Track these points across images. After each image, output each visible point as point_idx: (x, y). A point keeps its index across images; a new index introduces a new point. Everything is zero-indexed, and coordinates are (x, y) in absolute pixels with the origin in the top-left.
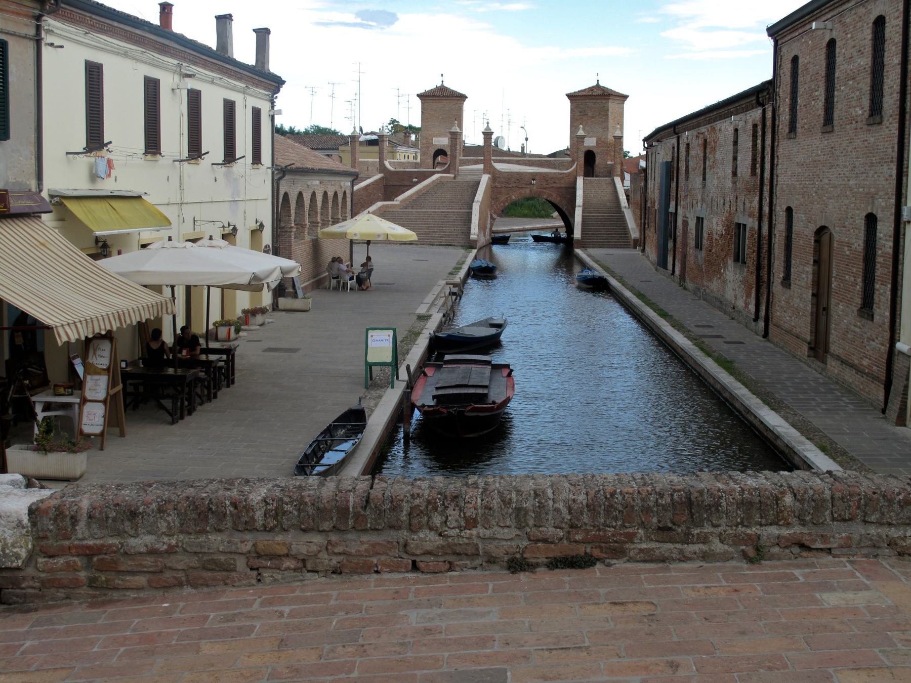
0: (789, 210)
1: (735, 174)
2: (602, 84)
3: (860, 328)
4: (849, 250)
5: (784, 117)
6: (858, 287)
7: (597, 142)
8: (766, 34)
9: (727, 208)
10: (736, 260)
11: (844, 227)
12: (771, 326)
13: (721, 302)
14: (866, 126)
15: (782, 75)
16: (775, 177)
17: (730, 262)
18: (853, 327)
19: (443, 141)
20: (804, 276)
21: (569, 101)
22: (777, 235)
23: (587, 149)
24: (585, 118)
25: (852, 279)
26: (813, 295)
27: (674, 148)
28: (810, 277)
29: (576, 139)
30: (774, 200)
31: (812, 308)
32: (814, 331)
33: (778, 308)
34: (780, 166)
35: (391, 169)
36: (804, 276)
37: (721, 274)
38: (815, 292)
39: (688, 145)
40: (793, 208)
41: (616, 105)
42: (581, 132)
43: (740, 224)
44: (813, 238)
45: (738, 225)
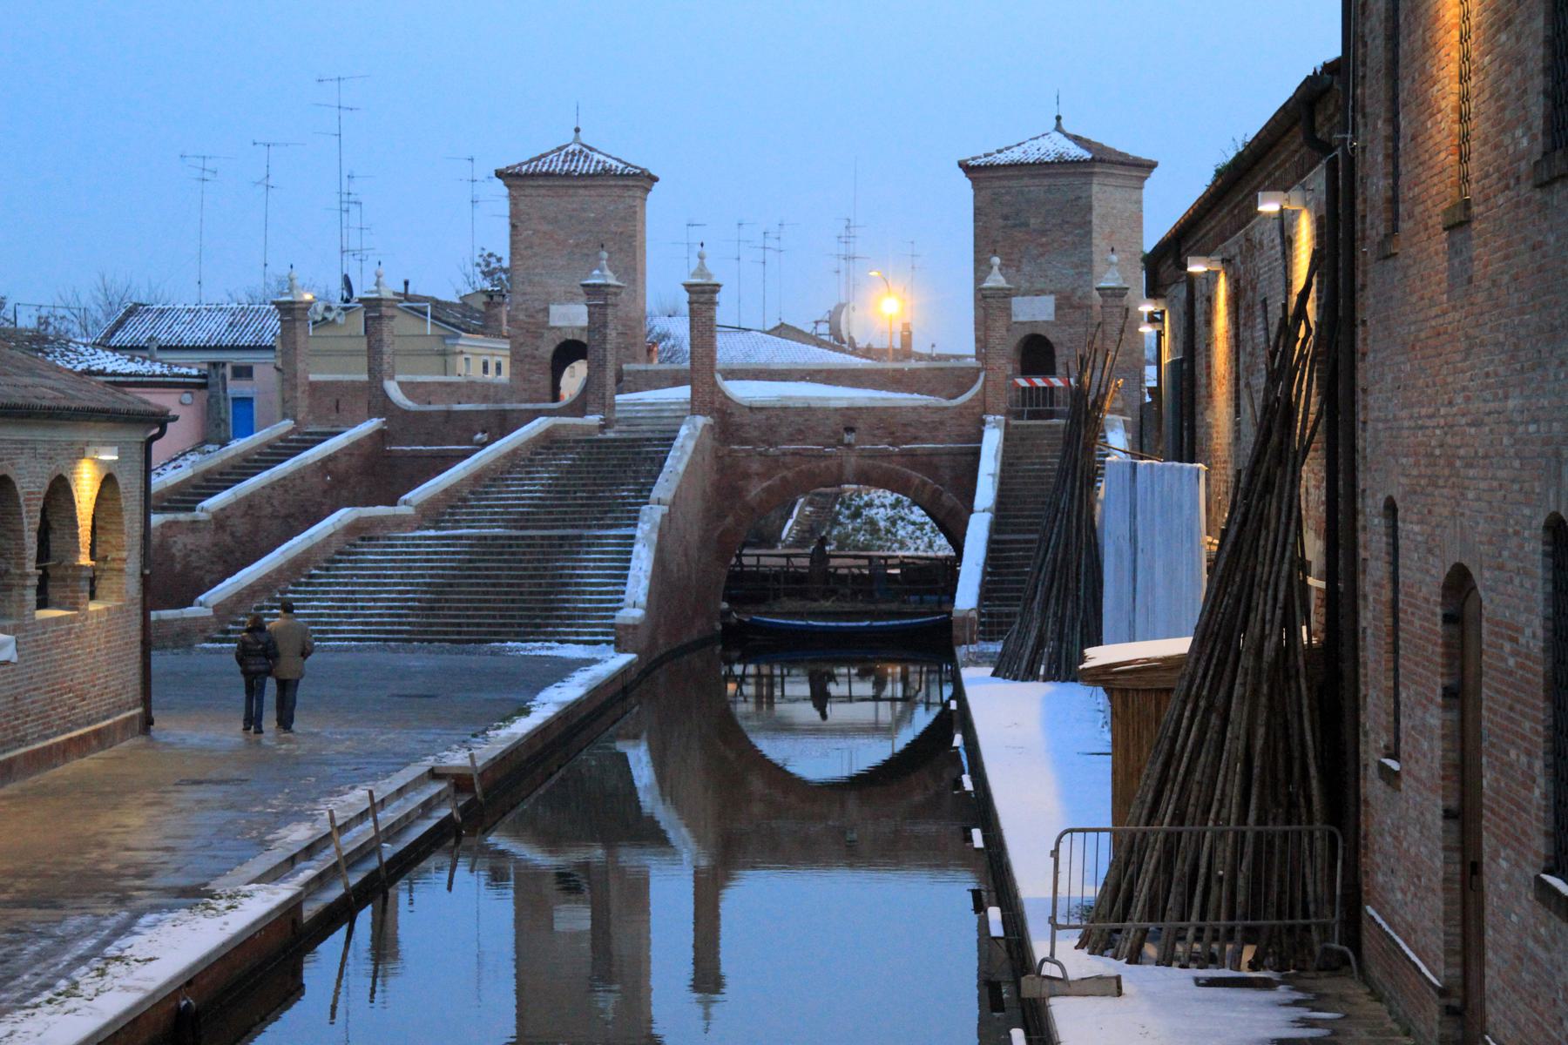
0: (1391, 508)
3: (1547, 949)
4: (1515, 653)
5: (1376, 186)
6: (1537, 792)
7: (1058, 307)
11: (1501, 568)
14: (1538, 195)
16: (1360, 395)
18: (1531, 943)
19: (571, 317)
21: (969, 183)
22: (1371, 598)
23: (1028, 331)
24: (1018, 234)
25: (1524, 759)
26: (1448, 814)
28: (1438, 746)
29: (989, 304)
30: (1360, 476)
31: (1446, 862)
32: (1458, 946)
33: (1378, 858)
34: (1371, 357)
35: (408, 404)
36: (1426, 746)
38: (1453, 803)
40: (1399, 504)
41: (1118, 194)
42: (996, 280)
44: (1439, 610)
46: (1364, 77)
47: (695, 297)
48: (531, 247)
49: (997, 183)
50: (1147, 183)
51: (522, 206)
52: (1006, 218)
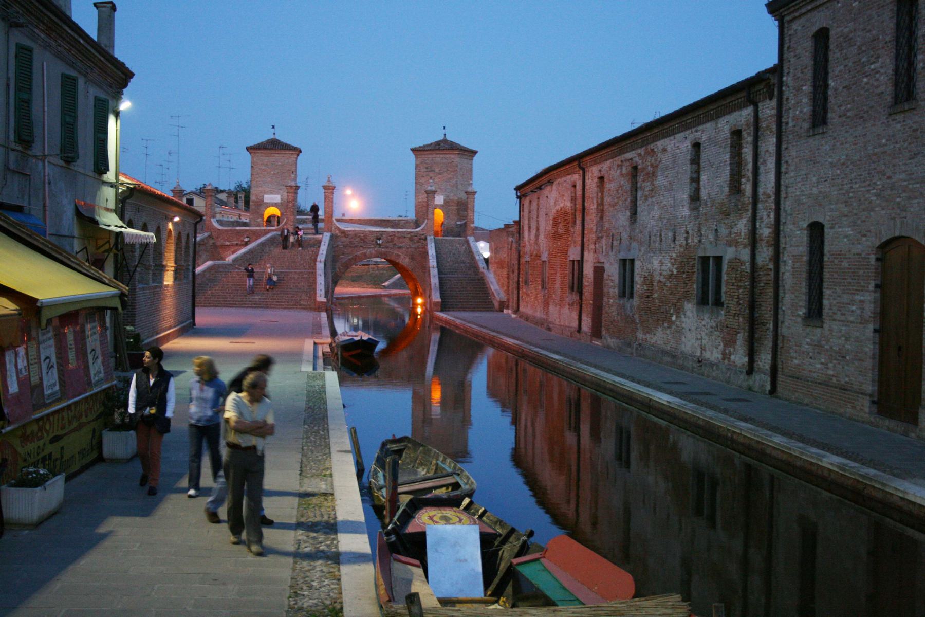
1: (695, 198)
2: (449, 138)
7: (444, 200)
8: (765, 9)
9: (681, 240)
10: (703, 301)
12: (780, 378)
13: (674, 357)
15: (793, 60)
16: (783, 188)
17: (689, 307)
20: (854, 308)
21: (414, 156)
24: (431, 174)
26: (875, 331)
27: (575, 186)
33: (793, 354)
34: (792, 174)
35: (220, 228)
37: (671, 323)
39: (601, 178)
41: (466, 161)
43: (708, 258)
45: (705, 260)
46: (788, 73)
47: (326, 191)
48: (258, 174)
49: (423, 156)
50: (475, 158)
51: (255, 160)
52: (427, 168)
